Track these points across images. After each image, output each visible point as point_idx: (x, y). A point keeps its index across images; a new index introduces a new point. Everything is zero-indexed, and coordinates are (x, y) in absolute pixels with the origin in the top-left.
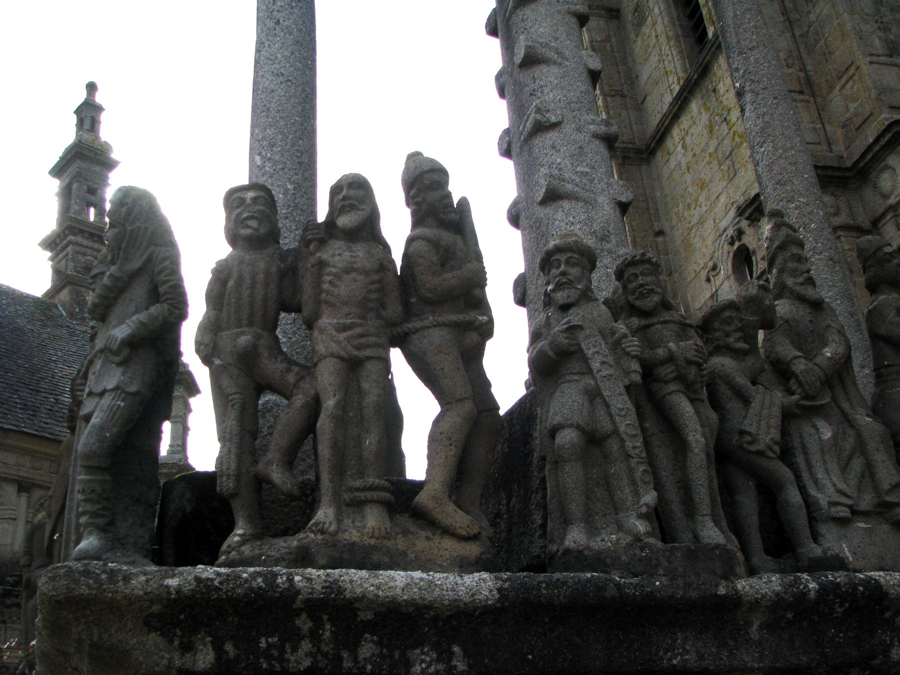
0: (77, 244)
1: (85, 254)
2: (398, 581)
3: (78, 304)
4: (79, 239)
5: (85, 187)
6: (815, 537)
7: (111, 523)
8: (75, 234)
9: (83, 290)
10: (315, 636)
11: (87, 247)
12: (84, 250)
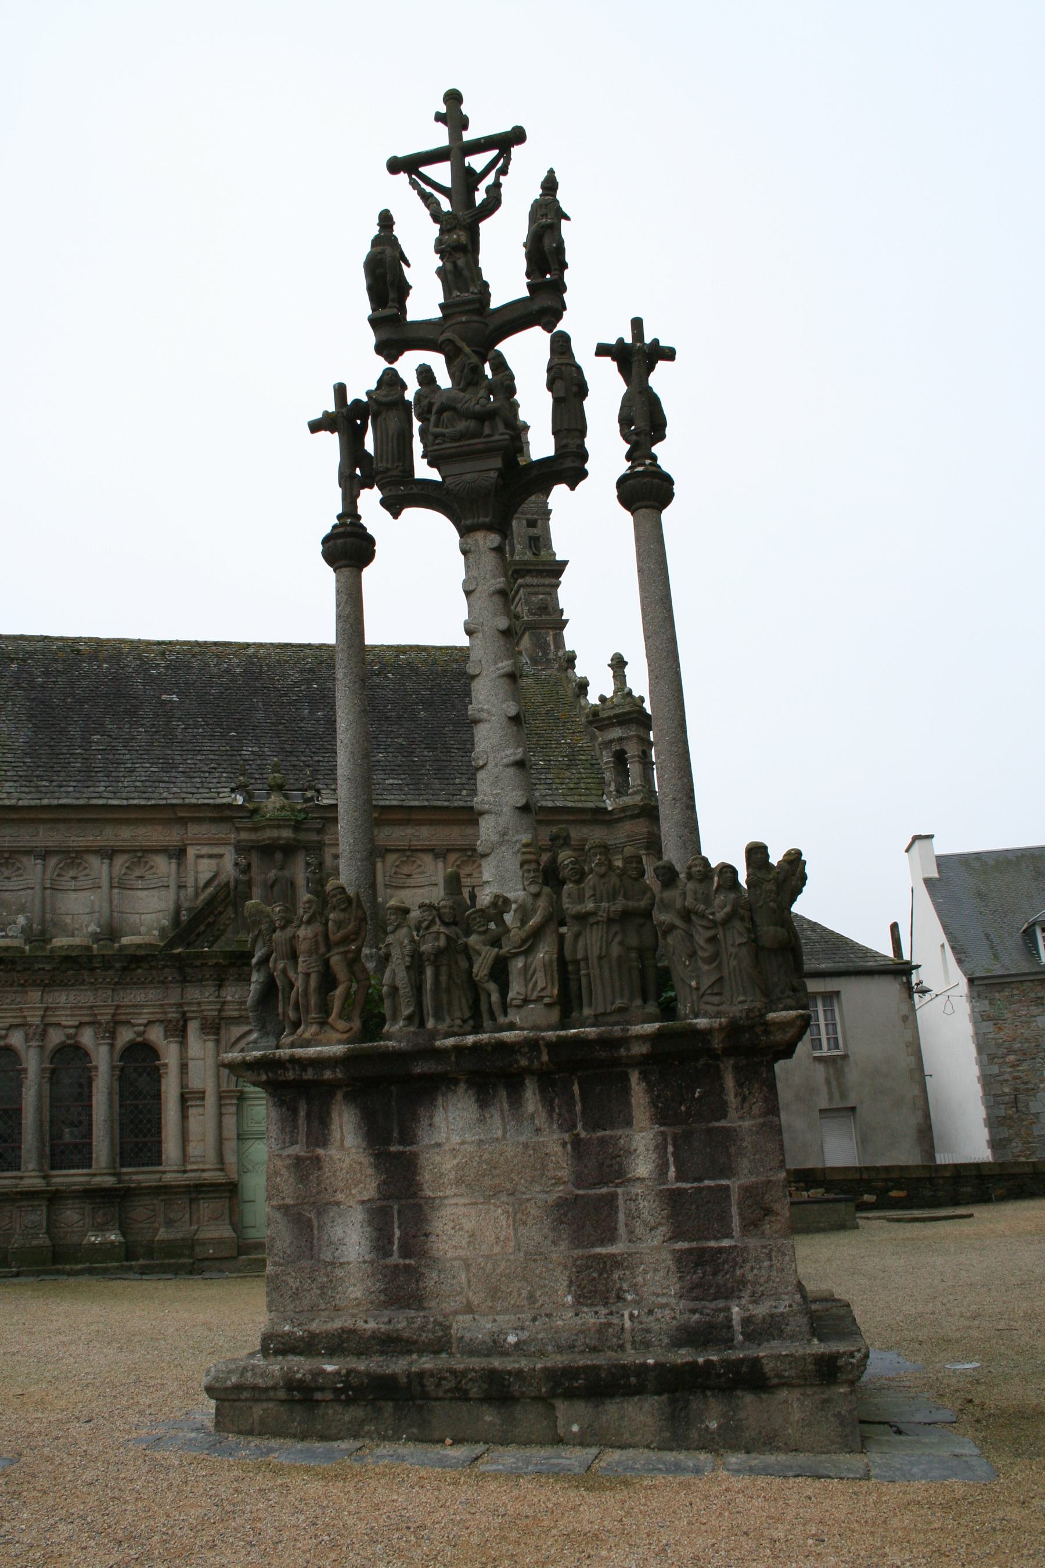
0: (527, 586)
1: (537, 593)
2: (312, 1051)
3: (540, 647)
4: (528, 580)
5: (524, 522)
6: (506, 1014)
7: (262, 1028)
8: (523, 577)
9: (544, 631)
10: (294, 1069)
11: (538, 586)
12: (536, 589)
